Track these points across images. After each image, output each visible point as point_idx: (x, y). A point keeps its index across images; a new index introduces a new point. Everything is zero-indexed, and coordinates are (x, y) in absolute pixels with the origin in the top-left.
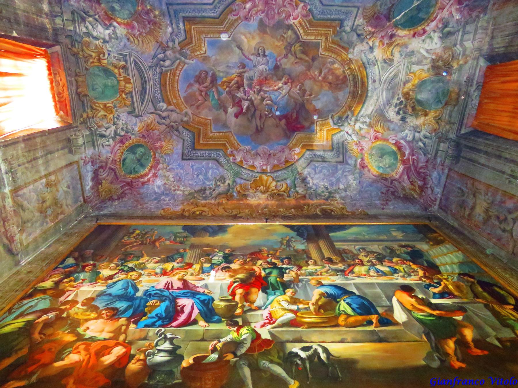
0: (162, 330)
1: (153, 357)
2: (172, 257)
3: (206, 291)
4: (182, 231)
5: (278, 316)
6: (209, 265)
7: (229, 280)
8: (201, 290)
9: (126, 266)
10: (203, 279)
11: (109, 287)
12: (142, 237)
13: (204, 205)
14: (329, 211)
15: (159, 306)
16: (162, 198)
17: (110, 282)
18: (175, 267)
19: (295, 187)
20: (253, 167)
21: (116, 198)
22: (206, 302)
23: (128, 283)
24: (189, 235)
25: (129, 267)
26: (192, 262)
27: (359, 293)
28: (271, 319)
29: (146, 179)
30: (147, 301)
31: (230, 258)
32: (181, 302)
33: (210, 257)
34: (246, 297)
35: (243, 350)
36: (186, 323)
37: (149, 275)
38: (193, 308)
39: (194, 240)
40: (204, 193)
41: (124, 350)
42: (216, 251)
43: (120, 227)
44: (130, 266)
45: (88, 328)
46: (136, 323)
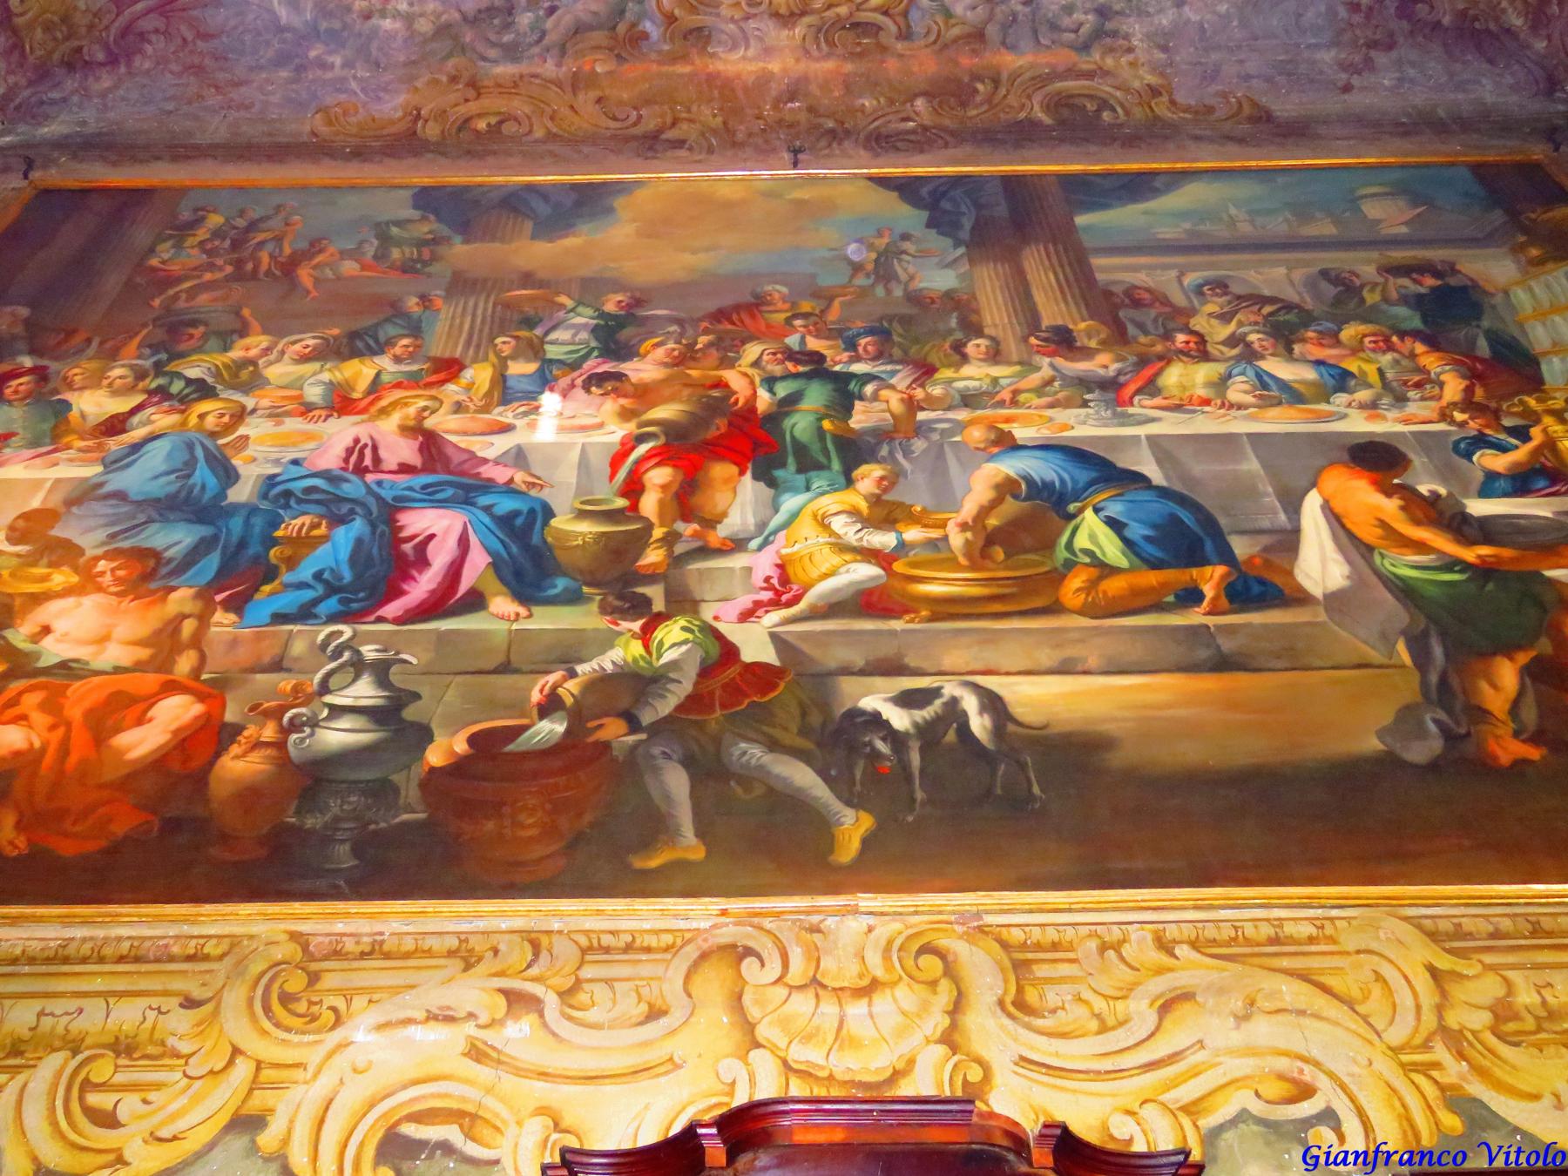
0: (341, 633)
1: (312, 734)
2: (372, 332)
3: (520, 477)
5: (814, 573)
6: (531, 367)
7: (616, 433)
8: (500, 475)
9: (179, 375)
10: (506, 429)
11: (113, 464)
12: (236, 245)
13: (512, 87)
14: (1091, 106)
15: (324, 539)
16: (313, 54)
17: (115, 444)
18: (385, 378)
21: (101, 56)
22: (519, 521)
23: (190, 447)
24: (444, 230)
25: (189, 382)
26: (458, 354)
27: (1167, 478)
28: (783, 588)
30: (275, 523)
31: (626, 333)
32: (417, 522)
33: (538, 331)
34: (684, 502)
35: (665, 706)
36: (435, 607)
37: (276, 415)
38: (464, 543)
39: (461, 252)
40: (507, 26)
41: (198, 709)
42: (562, 306)
43: (138, 197)
44: (193, 373)
45: (46, 630)
46: (237, 605)
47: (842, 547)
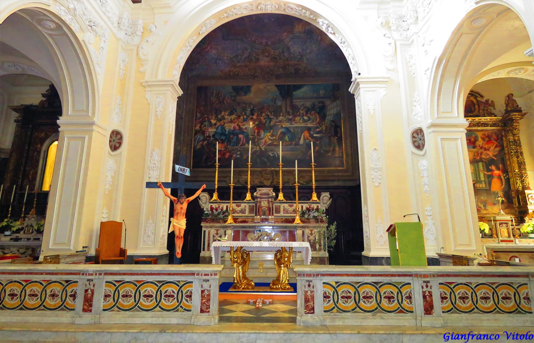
4: (232, 91)
19: (284, 52)
20: (261, 43)
29: (207, 50)
36: (242, 145)
46: (229, 145)
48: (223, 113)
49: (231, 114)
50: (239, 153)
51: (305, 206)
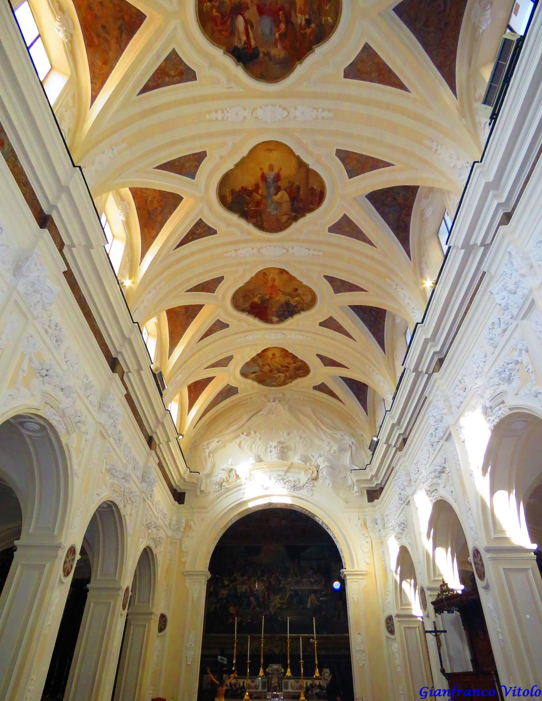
47: (279, 602)
48: (235, 575)
49: (242, 575)
50: (249, 617)
51: (309, 682)
